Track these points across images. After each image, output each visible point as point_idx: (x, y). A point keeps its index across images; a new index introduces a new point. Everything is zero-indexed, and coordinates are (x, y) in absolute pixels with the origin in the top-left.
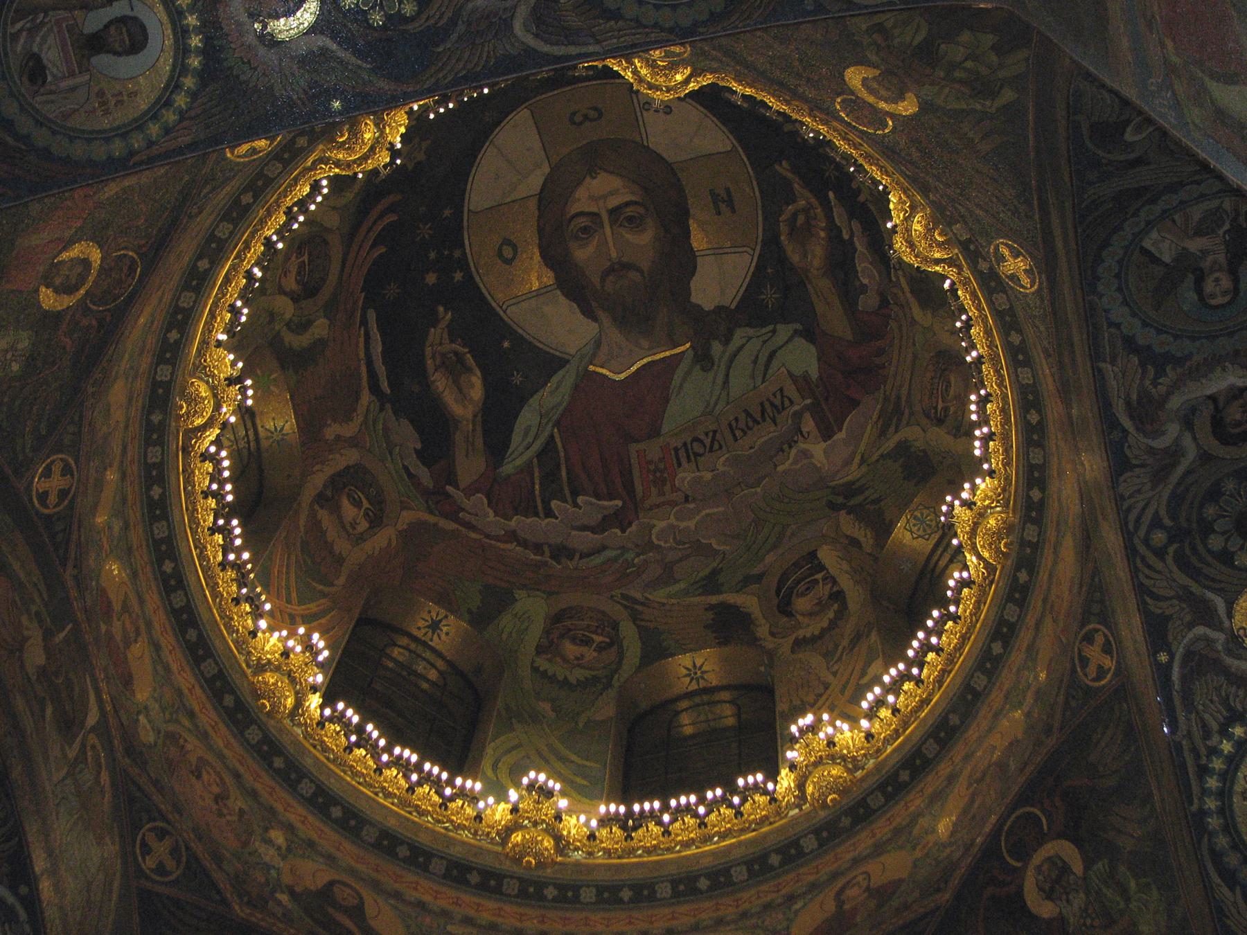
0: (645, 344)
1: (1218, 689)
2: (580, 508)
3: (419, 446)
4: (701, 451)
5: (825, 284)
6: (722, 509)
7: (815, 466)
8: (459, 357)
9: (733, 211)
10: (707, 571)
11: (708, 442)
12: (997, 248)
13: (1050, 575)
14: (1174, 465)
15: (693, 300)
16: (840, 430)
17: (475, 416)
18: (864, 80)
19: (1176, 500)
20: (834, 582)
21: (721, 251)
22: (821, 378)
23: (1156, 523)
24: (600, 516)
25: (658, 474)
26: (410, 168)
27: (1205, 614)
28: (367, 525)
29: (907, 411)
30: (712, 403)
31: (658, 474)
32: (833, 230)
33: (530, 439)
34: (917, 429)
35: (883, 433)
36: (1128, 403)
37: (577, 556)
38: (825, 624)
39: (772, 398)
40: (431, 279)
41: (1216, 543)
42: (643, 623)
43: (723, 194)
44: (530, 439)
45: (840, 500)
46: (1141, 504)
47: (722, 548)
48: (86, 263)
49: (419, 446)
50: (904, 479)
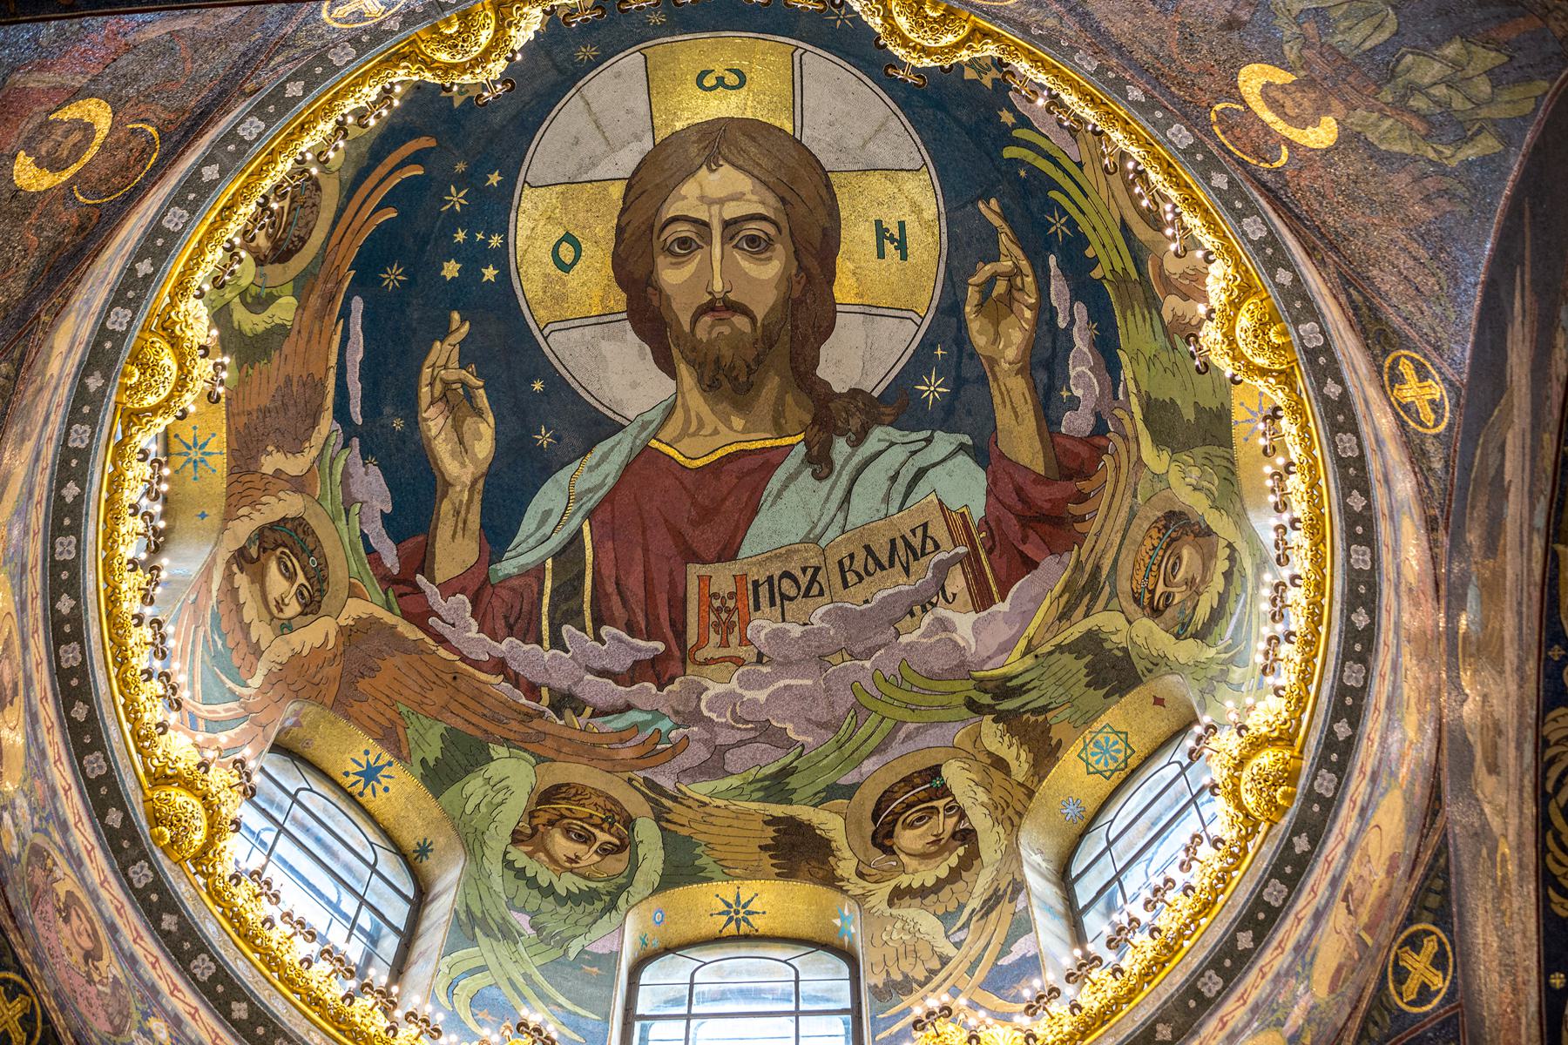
0: (738, 422)
2: (603, 643)
3: (388, 509)
4: (792, 592)
5: (1018, 386)
6: (809, 682)
7: (956, 644)
8: (469, 396)
9: (904, 257)
10: (773, 769)
11: (804, 581)
12: (1396, 361)
13: (1350, 847)
15: (821, 372)
16: (1003, 599)
17: (474, 482)
18: (1268, 85)
20: (963, 815)
21: (874, 311)
22: (985, 521)
24: (629, 662)
25: (724, 616)
26: (456, 105)
28: (298, 609)
29: (1107, 589)
30: (821, 525)
31: (724, 616)
32: (1045, 311)
33: (547, 529)
34: (1120, 621)
35: (1065, 615)
37: (588, 711)
38: (943, 872)
39: (909, 536)
40: (451, 269)
42: (669, 826)
43: (896, 233)
44: (547, 529)
45: (986, 699)
47: (801, 738)
48: (88, 129)
49: (388, 509)
50: (1088, 685)
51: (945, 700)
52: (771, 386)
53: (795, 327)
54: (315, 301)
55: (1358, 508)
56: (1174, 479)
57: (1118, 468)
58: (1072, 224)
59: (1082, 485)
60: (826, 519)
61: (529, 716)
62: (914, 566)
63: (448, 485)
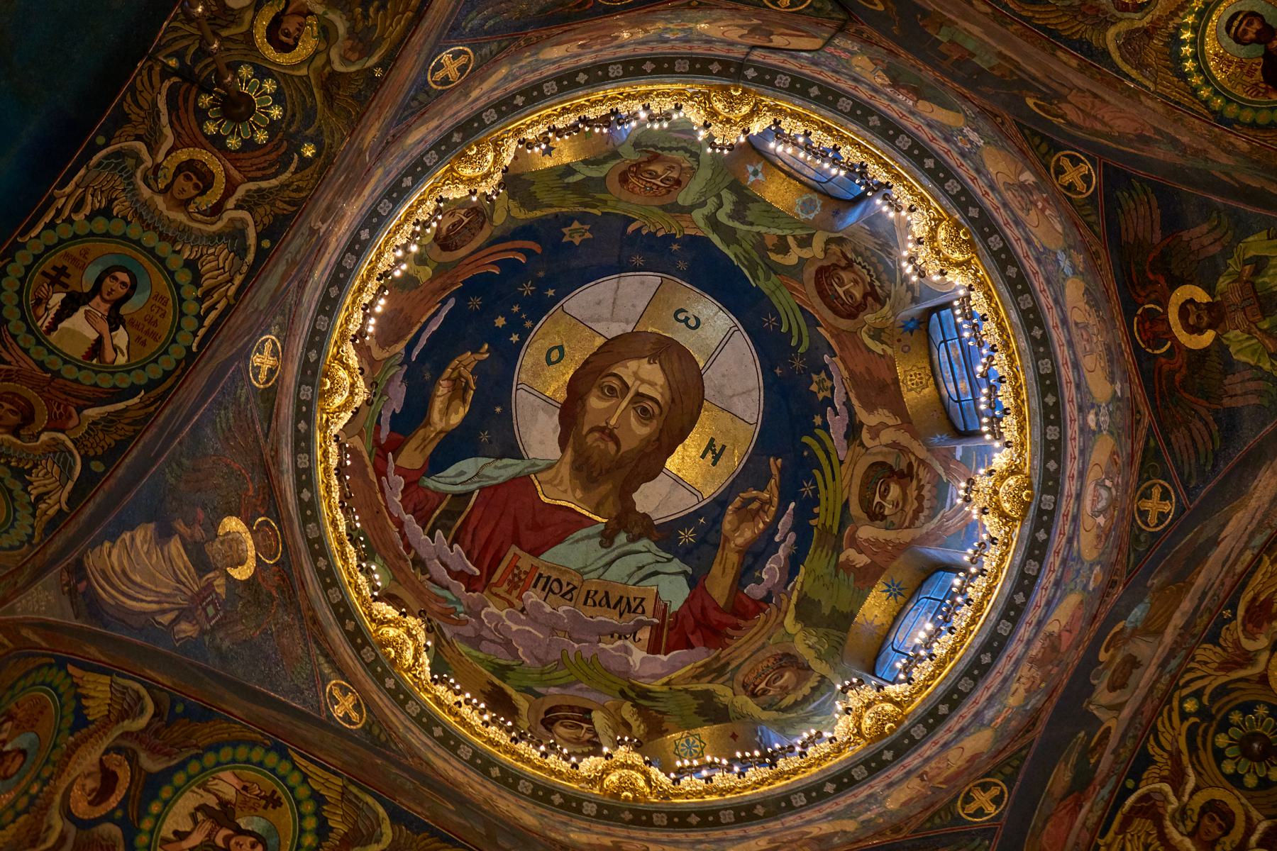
0: (579, 494)
1: (1148, 834)
5: (734, 558)
8: (466, 389)
10: (503, 662)
11: (565, 589)
14: (1241, 666)
15: (636, 496)
17: (441, 432)
19: (1222, 691)
20: (596, 735)
22: (676, 613)
23: (1198, 694)
24: (459, 568)
26: (564, 240)
27: (1177, 780)
32: (772, 529)
34: (729, 692)
36: (1254, 599)
40: (500, 322)
41: (1222, 740)
43: (718, 449)
44: (458, 480)
45: (632, 694)
46: (1199, 674)
49: (398, 411)
51: (608, 683)
52: (605, 488)
53: (636, 466)
54: (438, 283)
55: (1018, 602)
56: (797, 639)
57: (766, 622)
58: (816, 491)
59: (741, 622)
60: (593, 567)
61: (400, 557)
62: (626, 615)
63: (429, 423)
